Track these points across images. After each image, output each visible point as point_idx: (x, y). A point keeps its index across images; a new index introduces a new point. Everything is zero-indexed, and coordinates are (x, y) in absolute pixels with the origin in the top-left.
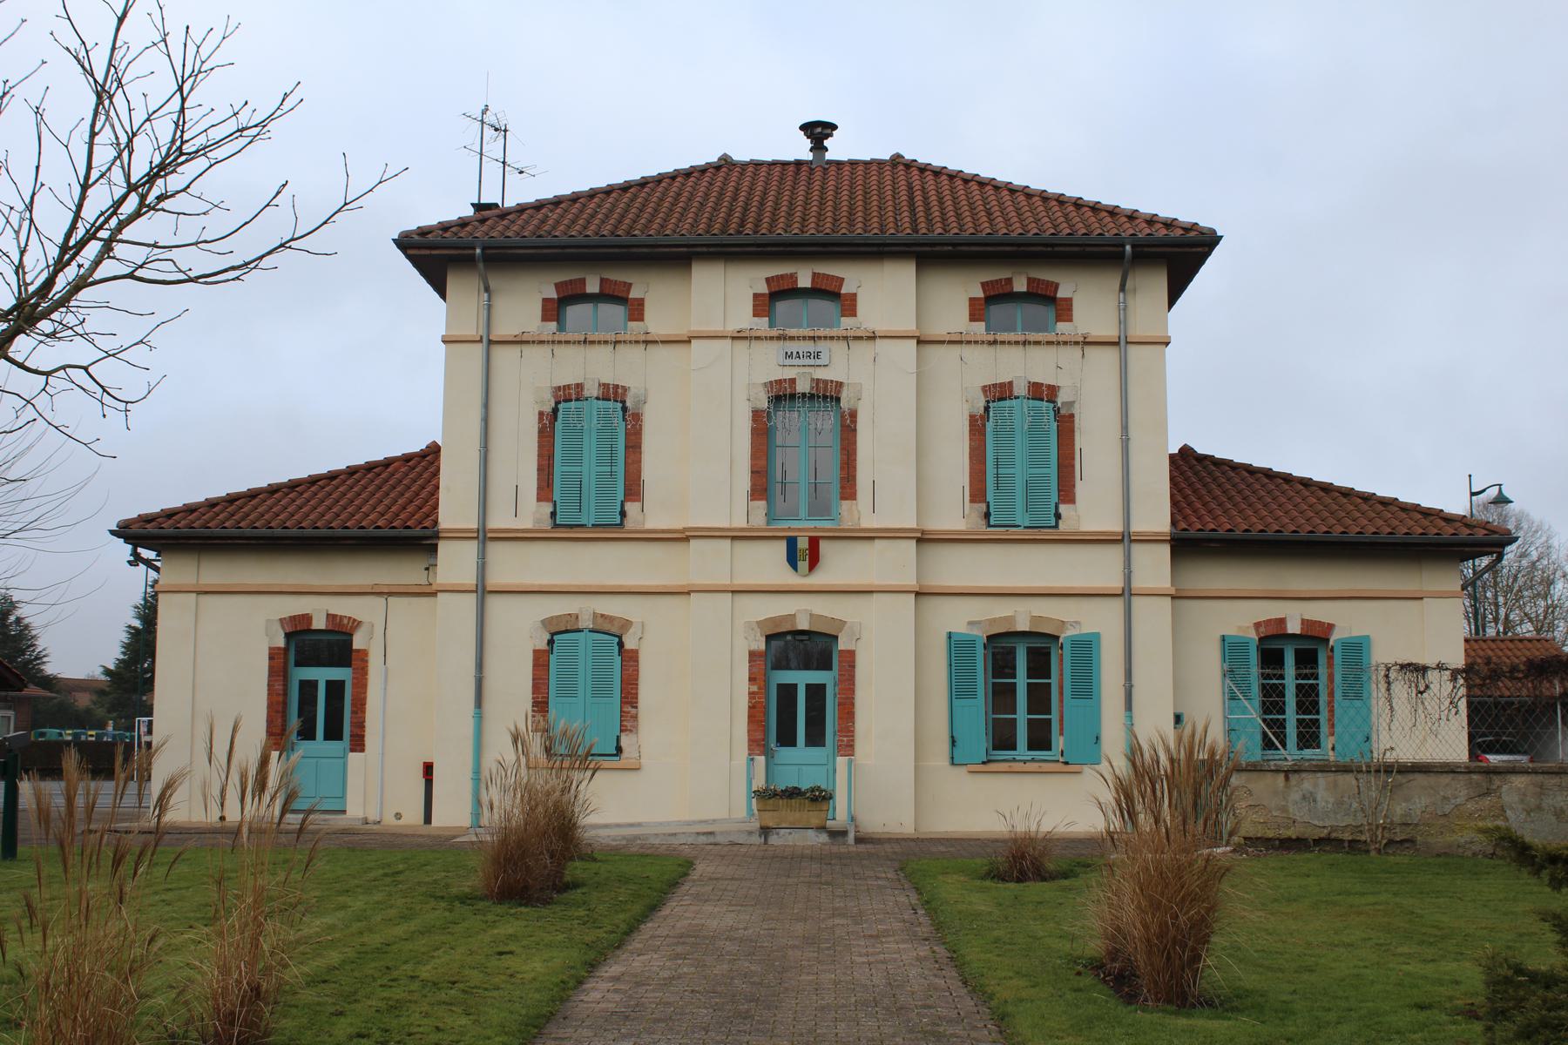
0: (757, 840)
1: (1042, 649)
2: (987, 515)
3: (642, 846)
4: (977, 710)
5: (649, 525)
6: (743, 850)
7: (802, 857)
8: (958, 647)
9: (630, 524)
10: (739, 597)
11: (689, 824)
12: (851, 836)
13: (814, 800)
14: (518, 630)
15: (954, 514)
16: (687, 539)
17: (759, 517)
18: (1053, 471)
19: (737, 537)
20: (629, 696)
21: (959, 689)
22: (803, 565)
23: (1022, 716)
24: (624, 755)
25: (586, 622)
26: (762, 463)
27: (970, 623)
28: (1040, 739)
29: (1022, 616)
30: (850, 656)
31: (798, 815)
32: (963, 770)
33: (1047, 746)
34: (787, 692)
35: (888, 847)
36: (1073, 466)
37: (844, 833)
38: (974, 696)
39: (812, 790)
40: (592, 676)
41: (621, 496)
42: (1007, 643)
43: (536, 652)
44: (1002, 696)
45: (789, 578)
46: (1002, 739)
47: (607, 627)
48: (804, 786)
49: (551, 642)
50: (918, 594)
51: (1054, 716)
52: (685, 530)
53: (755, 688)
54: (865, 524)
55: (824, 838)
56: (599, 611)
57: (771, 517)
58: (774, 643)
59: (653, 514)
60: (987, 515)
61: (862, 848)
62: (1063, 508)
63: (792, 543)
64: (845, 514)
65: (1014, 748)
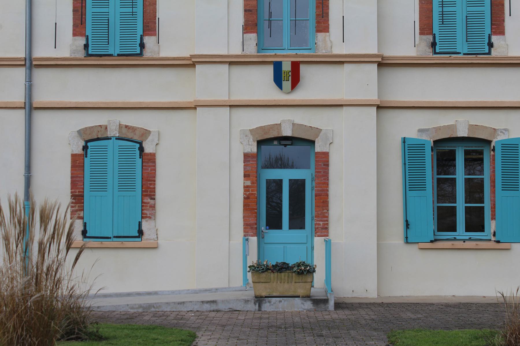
0: (252, 307)
1: (476, 149)
2: (434, 45)
3: (155, 315)
4: (426, 203)
5: (163, 55)
6: (241, 317)
7: (294, 325)
8: (411, 150)
9: (147, 53)
10: (235, 111)
11: (196, 292)
12: (332, 303)
13: (300, 273)
14: (58, 138)
15: (407, 44)
16: (193, 65)
17: (251, 49)
18: (487, 9)
19: (234, 62)
20: (149, 190)
21: (412, 183)
22: (287, 84)
23: (461, 205)
24: (145, 237)
25: (113, 132)
26: (255, 3)
27: (421, 131)
28: (475, 223)
29: (462, 125)
30: (323, 160)
31: (286, 286)
32: (415, 247)
33: (481, 228)
34: (274, 187)
35: (363, 312)
36: (503, 5)
37: (326, 301)
38: (423, 188)
39: (299, 265)
40: (118, 174)
41: (140, 32)
42: (447, 148)
43: (74, 156)
44: (444, 190)
45: (275, 95)
46: (445, 221)
47: (130, 135)
48: (291, 262)
49: (85, 148)
50: (379, 107)
51: (487, 205)
52: (192, 56)
53: (249, 183)
54: (336, 51)
55: (308, 305)
56: (124, 123)
57: (260, 46)
58: (263, 147)
59: (167, 45)
60: (434, 45)
61: (342, 314)
62: (495, 39)
63: (277, 66)
64: (320, 43)
65: (455, 230)
